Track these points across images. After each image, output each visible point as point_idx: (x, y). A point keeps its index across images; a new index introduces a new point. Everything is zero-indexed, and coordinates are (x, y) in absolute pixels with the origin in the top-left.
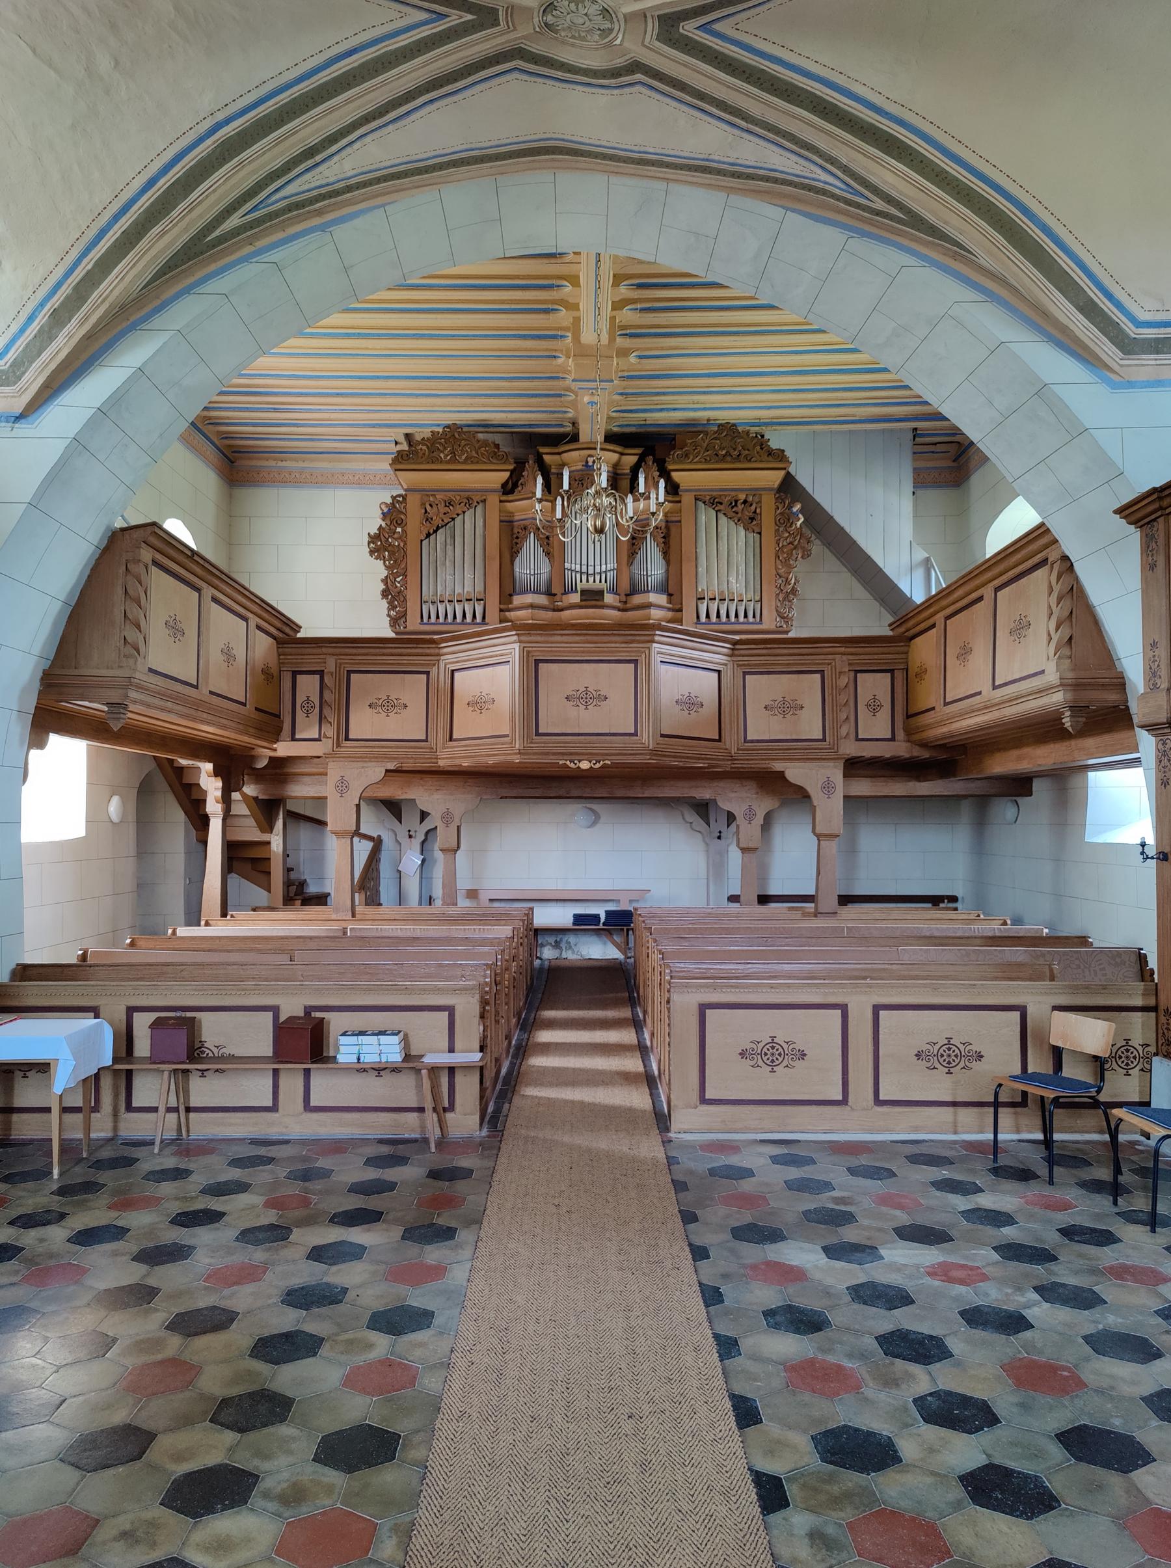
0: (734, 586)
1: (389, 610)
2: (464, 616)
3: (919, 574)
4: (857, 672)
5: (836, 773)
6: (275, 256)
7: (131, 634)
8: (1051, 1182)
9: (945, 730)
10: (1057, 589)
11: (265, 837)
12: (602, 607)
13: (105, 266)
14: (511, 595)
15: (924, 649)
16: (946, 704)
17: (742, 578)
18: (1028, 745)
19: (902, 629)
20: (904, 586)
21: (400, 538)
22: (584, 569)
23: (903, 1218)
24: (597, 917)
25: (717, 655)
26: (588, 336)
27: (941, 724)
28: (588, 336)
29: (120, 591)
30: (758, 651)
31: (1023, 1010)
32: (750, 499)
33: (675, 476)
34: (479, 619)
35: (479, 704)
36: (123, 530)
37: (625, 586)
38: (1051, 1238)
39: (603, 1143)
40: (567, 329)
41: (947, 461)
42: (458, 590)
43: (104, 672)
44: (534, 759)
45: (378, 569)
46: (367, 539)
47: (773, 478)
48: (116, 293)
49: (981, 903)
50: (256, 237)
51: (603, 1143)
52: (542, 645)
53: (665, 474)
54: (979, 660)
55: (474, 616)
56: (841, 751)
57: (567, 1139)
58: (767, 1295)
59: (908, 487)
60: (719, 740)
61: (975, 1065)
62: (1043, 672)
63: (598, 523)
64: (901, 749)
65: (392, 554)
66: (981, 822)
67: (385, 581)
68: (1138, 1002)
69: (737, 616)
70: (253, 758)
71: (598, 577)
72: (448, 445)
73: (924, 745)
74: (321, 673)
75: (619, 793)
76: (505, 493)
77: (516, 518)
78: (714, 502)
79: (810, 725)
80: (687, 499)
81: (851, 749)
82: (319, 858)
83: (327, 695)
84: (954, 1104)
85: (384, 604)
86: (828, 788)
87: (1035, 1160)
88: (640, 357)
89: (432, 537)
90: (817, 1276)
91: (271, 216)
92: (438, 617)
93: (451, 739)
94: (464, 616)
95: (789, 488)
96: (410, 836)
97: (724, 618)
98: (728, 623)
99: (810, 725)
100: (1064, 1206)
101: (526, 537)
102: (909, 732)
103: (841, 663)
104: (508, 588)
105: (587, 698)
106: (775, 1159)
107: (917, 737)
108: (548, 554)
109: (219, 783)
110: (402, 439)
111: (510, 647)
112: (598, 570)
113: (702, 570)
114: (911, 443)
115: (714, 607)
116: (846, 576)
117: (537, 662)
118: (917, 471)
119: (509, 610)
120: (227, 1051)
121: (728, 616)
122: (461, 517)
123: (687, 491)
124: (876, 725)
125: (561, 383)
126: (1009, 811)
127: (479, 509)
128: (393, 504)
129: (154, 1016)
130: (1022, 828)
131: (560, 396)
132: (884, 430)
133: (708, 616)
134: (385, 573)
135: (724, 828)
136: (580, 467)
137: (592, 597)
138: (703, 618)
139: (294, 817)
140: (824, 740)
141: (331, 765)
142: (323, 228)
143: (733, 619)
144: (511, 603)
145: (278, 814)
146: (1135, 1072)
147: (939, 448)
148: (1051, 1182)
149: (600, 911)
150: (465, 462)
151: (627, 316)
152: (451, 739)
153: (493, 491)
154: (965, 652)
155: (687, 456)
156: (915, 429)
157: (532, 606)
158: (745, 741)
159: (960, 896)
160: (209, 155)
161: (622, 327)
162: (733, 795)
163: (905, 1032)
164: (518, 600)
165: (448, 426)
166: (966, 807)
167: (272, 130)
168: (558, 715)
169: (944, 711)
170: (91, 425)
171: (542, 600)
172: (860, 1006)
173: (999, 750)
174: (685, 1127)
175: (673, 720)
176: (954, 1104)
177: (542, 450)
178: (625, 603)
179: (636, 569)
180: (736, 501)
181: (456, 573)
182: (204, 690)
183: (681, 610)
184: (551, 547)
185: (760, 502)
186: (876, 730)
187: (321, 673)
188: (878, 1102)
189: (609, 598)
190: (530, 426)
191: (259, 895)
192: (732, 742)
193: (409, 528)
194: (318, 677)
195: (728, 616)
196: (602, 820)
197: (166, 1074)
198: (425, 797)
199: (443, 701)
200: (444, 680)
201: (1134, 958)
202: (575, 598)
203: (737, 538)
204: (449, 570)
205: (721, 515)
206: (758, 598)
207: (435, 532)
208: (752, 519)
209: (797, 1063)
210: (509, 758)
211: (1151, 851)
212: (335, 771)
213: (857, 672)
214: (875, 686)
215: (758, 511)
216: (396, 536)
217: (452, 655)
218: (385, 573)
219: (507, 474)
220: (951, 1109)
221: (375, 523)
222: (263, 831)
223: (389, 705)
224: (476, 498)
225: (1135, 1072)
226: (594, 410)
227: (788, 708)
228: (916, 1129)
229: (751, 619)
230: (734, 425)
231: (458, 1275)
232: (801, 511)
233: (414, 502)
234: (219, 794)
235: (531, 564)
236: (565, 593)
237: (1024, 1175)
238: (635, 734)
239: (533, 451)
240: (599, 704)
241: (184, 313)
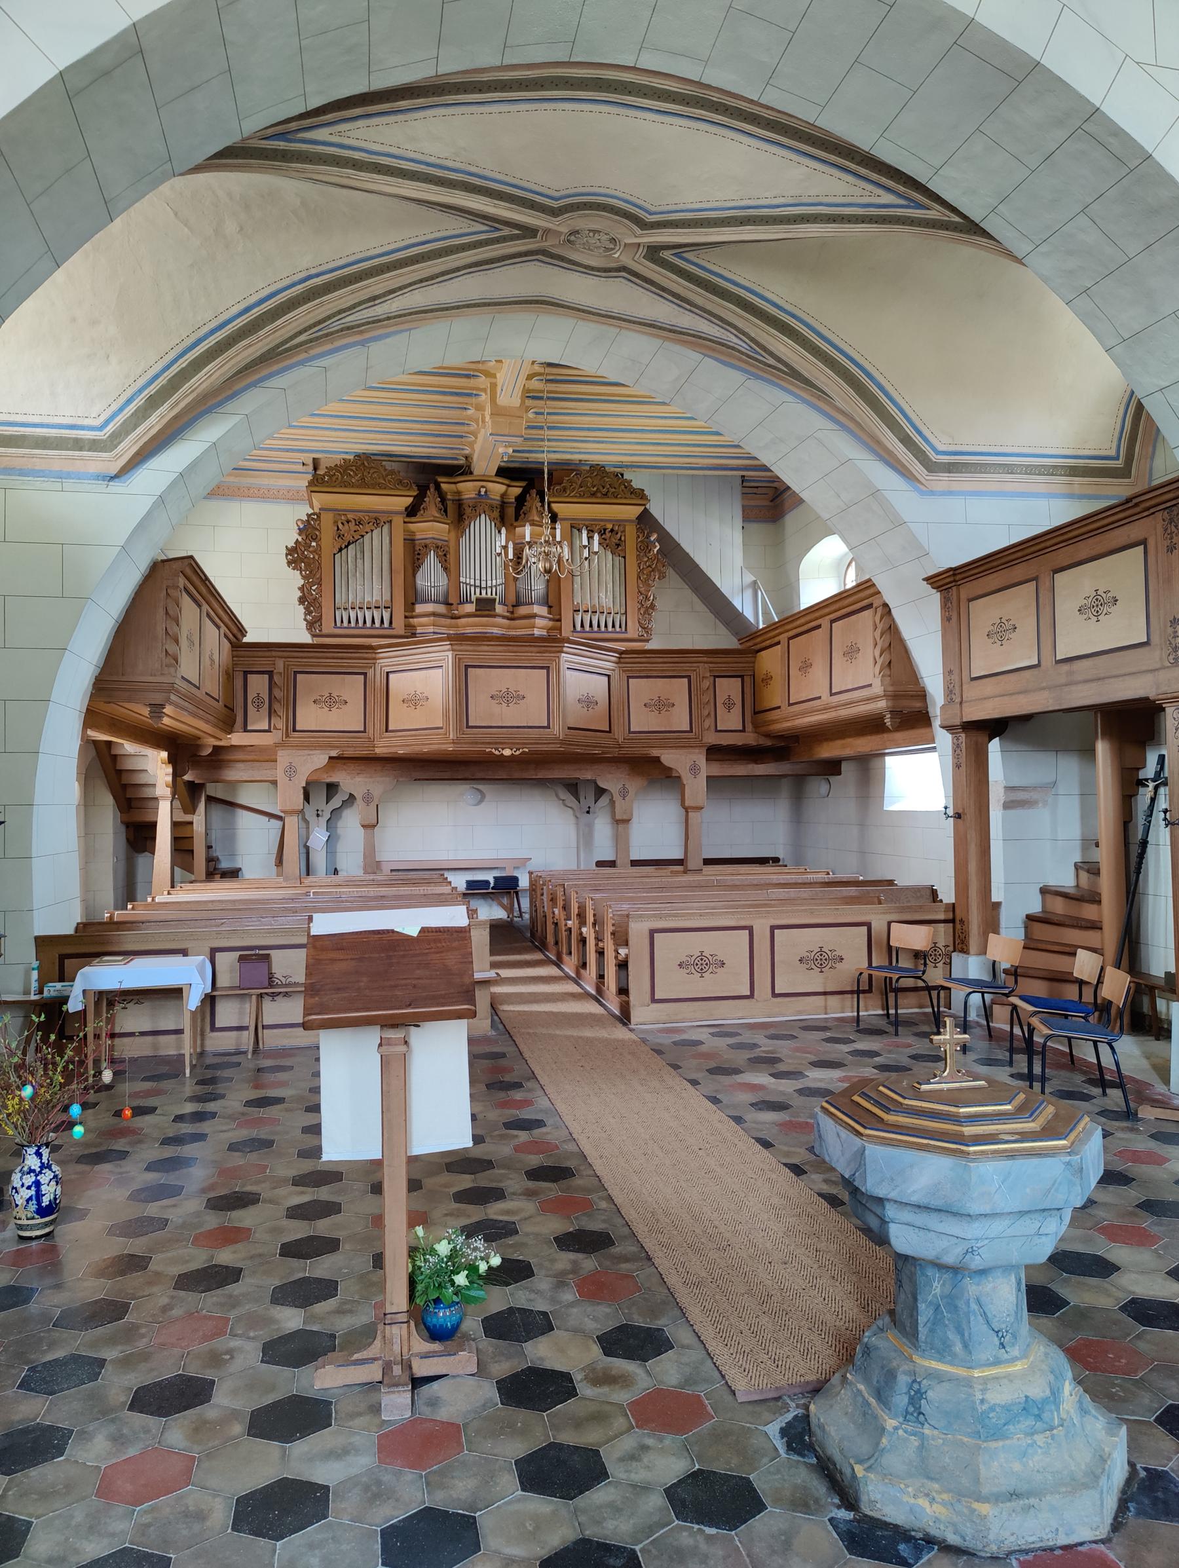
1: (306, 615)
3: (748, 594)
4: (715, 677)
5: (700, 758)
6: (326, 362)
7: (172, 648)
8: (897, 1034)
9: (789, 724)
10: (880, 627)
11: (188, 818)
12: (495, 616)
13: (198, 365)
14: (413, 604)
15: (769, 661)
16: (790, 705)
18: (850, 736)
19: (749, 644)
20: (737, 603)
21: (315, 551)
22: (478, 583)
23: (813, 1058)
24: (487, 882)
25: (607, 663)
26: (503, 400)
27: (786, 719)
28: (503, 400)
29: (161, 612)
30: (639, 662)
31: (869, 925)
34: (386, 624)
35: (413, 701)
36: (163, 561)
37: (512, 599)
38: (905, 1061)
39: (588, 1033)
40: (485, 390)
41: (767, 502)
43: (151, 679)
44: (466, 748)
45: (295, 579)
46: (285, 551)
47: (636, 511)
48: (204, 386)
49: (799, 860)
50: (311, 348)
51: (588, 1033)
52: (470, 653)
54: (818, 673)
55: (382, 622)
56: (705, 740)
57: (558, 1032)
58: (747, 1097)
59: (739, 522)
60: (610, 732)
61: (838, 965)
62: (870, 685)
63: (547, 565)
64: (750, 739)
65: (308, 565)
66: (798, 798)
67: (301, 589)
68: (942, 917)
69: (606, 626)
70: (199, 747)
71: (489, 591)
73: (767, 735)
74: (270, 674)
75: (516, 775)
76: (408, 516)
77: (418, 537)
79: (680, 720)
81: (712, 739)
82: (230, 838)
83: (277, 693)
84: (825, 993)
85: (301, 609)
86: (694, 770)
87: (882, 1024)
88: (537, 413)
89: (344, 552)
90: (773, 1087)
91: (327, 335)
92: (349, 622)
93: (387, 731)
95: (646, 521)
96: (318, 815)
97: (595, 628)
98: (599, 631)
99: (680, 720)
100: (910, 1046)
102: (756, 726)
103: (704, 669)
104: (413, 597)
105: (509, 697)
106: (713, 1034)
107: (764, 729)
108: (445, 569)
109: (170, 770)
110: (310, 462)
111: (445, 655)
112: (489, 584)
113: (577, 586)
114: (740, 487)
115: (587, 618)
116: (688, 593)
117: (467, 667)
118: (744, 509)
119: (412, 617)
120: (292, 980)
121: (599, 626)
124: (731, 720)
125: (466, 428)
126: (824, 788)
127: (386, 528)
128: (308, 521)
129: (237, 954)
130: (832, 803)
131: (462, 437)
133: (582, 626)
134: (302, 582)
135: (592, 804)
137: (485, 606)
138: (579, 628)
139: (210, 799)
140: (691, 731)
141: (280, 753)
142: (363, 343)
143: (603, 628)
144: (413, 610)
145: (200, 797)
146: (940, 965)
147: (759, 491)
148: (897, 1034)
149: (489, 877)
151: (535, 384)
152: (387, 731)
154: (806, 666)
155: (565, 490)
156: (743, 476)
157: (434, 614)
158: (630, 732)
159: (781, 857)
160: (297, 296)
161: (529, 391)
162: (610, 776)
163: (793, 944)
164: (420, 608)
166: (786, 787)
167: (351, 283)
168: (484, 711)
169: (787, 710)
170: (173, 485)
171: (441, 609)
172: (762, 927)
173: (826, 740)
174: (641, 1020)
175: (576, 715)
176: (825, 993)
177: (440, 479)
178: (512, 613)
181: (365, 586)
182: (203, 690)
183: (559, 620)
185: (624, 531)
186: (730, 722)
187: (270, 674)
188: (775, 995)
189: (499, 609)
190: (428, 457)
191: (189, 868)
192: (619, 734)
193: (323, 543)
194: (266, 676)
195: (599, 626)
196: (488, 797)
197: (254, 997)
198: (350, 781)
199: (379, 698)
200: (380, 680)
201: (929, 892)
202: (470, 608)
207: (346, 547)
208: (618, 545)
209: (719, 970)
210: (443, 747)
211: (950, 812)
212: (284, 758)
213: (715, 677)
214: (729, 688)
217: (386, 660)
218: (302, 582)
220: (822, 997)
221: (292, 537)
222: (186, 811)
223: (331, 702)
225: (940, 965)
226: (488, 449)
227: (662, 705)
228: (800, 1013)
229: (618, 629)
231: (543, 1103)
232: (658, 540)
233: (327, 520)
234: (170, 779)
235: (431, 577)
236: (460, 603)
237: (879, 1032)
238: (548, 727)
239: (431, 482)
240: (517, 703)
241: (251, 401)
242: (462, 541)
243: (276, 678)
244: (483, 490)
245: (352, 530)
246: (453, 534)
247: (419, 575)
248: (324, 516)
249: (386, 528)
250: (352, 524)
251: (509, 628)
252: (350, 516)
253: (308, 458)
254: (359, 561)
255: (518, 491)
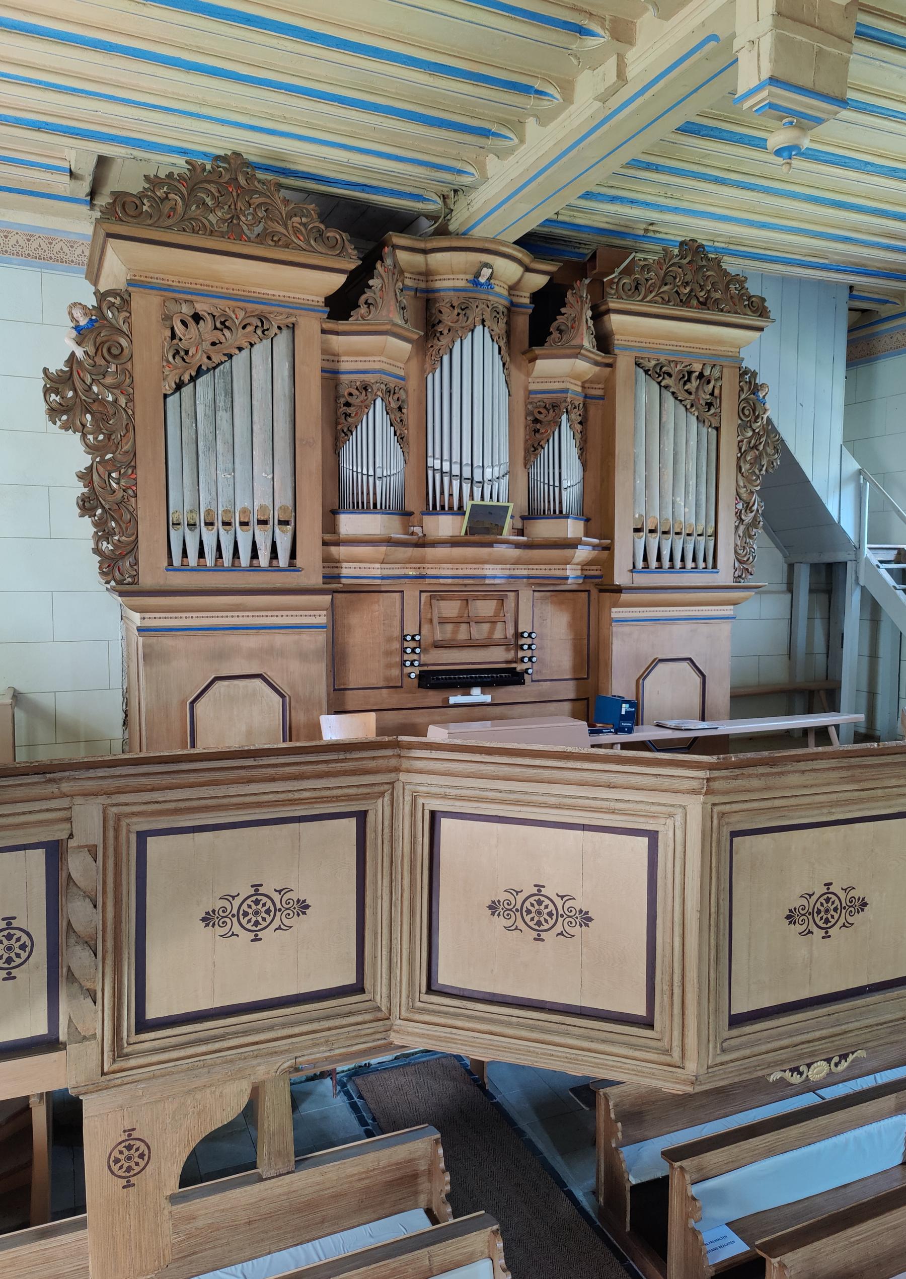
0: (681, 510)
1: (98, 539)
2: (255, 555)
3: (849, 492)
17: (692, 498)
20: (832, 508)
21: (117, 386)
22: (467, 473)
32: (707, 373)
33: (616, 321)
42: (242, 502)
53: (599, 315)
65: (101, 419)
67: (86, 476)
72: (218, 197)
76: (332, 316)
78: (658, 373)
80: (624, 362)
83: (79, 913)
85: (86, 527)
89: (187, 391)
92: (201, 554)
94: (255, 555)
101: (366, 406)
108: (401, 439)
110: (87, 168)
112: (488, 476)
119: (337, 544)
121: (671, 559)
122: (245, 353)
123: (625, 348)
127: (282, 341)
128: (99, 308)
132: (820, 283)
134: (87, 460)
136: (461, 284)
137: (484, 525)
138: (640, 564)
150: (261, 239)
153: (309, 309)
156: (851, 288)
165: (218, 158)
179: (540, 471)
180: (690, 373)
184: (410, 432)
185: (721, 378)
190: (364, 187)
200: (409, 835)
203: (685, 432)
204: (223, 461)
205: (667, 395)
206: (711, 531)
207: (193, 379)
208: (709, 405)
215: (717, 392)
216: (109, 380)
218: (87, 460)
219: (341, 279)
221: (60, 347)
223: (259, 911)
224: (281, 320)
230: (702, 246)
235: (376, 456)
242: (433, 381)
243: (77, 866)
244: (486, 272)
245: (205, 340)
246: (414, 365)
247: (348, 450)
248: (138, 302)
249: (282, 341)
250: (206, 326)
251: (518, 562)
252: (201, 307)
253: (80, 155)
254: (223, 416)
255: (540, 281)
